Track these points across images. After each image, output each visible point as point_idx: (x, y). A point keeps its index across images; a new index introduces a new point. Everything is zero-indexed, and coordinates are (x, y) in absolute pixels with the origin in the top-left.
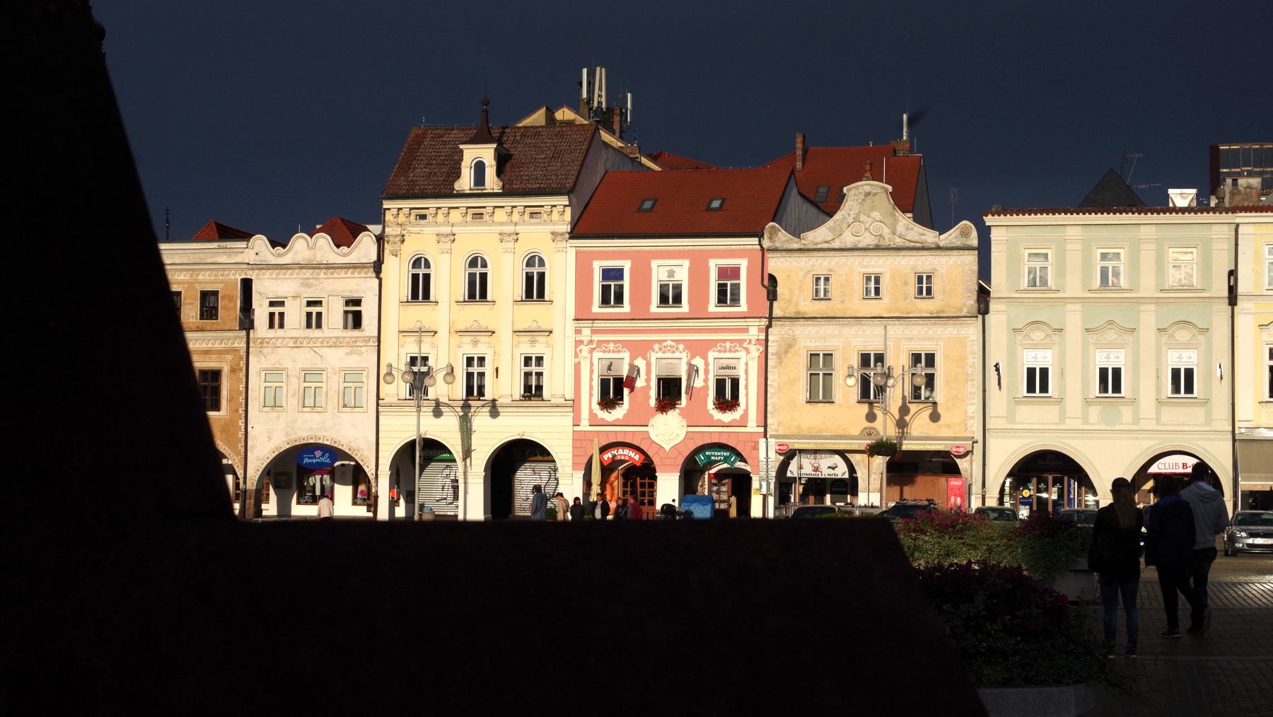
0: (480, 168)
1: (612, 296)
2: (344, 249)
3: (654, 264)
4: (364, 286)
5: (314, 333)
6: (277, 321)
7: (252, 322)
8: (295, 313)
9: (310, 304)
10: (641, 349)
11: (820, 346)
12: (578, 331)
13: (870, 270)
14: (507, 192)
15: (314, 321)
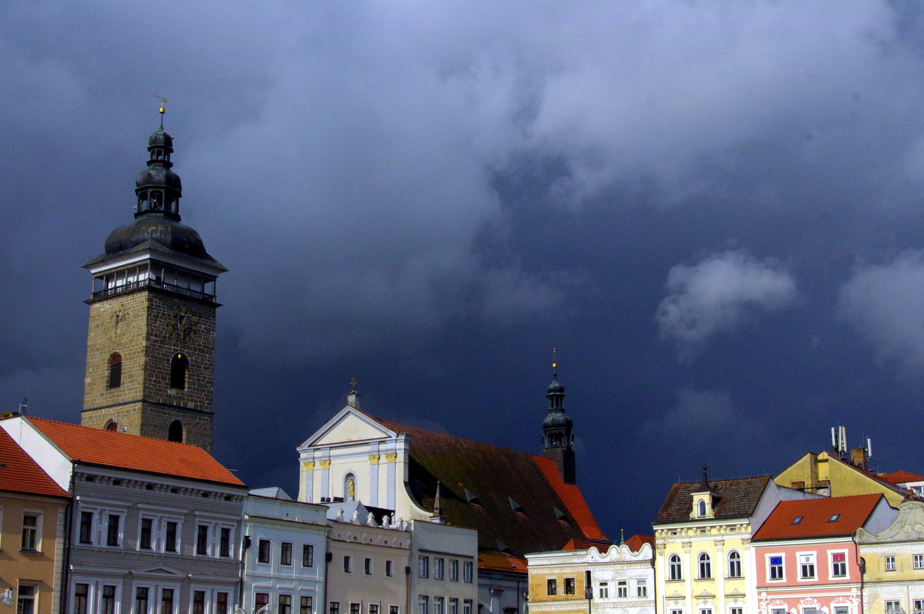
0: (703, 504)
1: (776, 573)
2: (636, 553)
3: (798, 554)
5: (623, 599)
6: (604, 594)
7: (591, 594)
8: (613, 589)
9: (620, 583)
10: (793, 603)
11: (892, 598)
12: (759, 594)
13: (916, 553)
14: (718, 517)
15: (622, 593)
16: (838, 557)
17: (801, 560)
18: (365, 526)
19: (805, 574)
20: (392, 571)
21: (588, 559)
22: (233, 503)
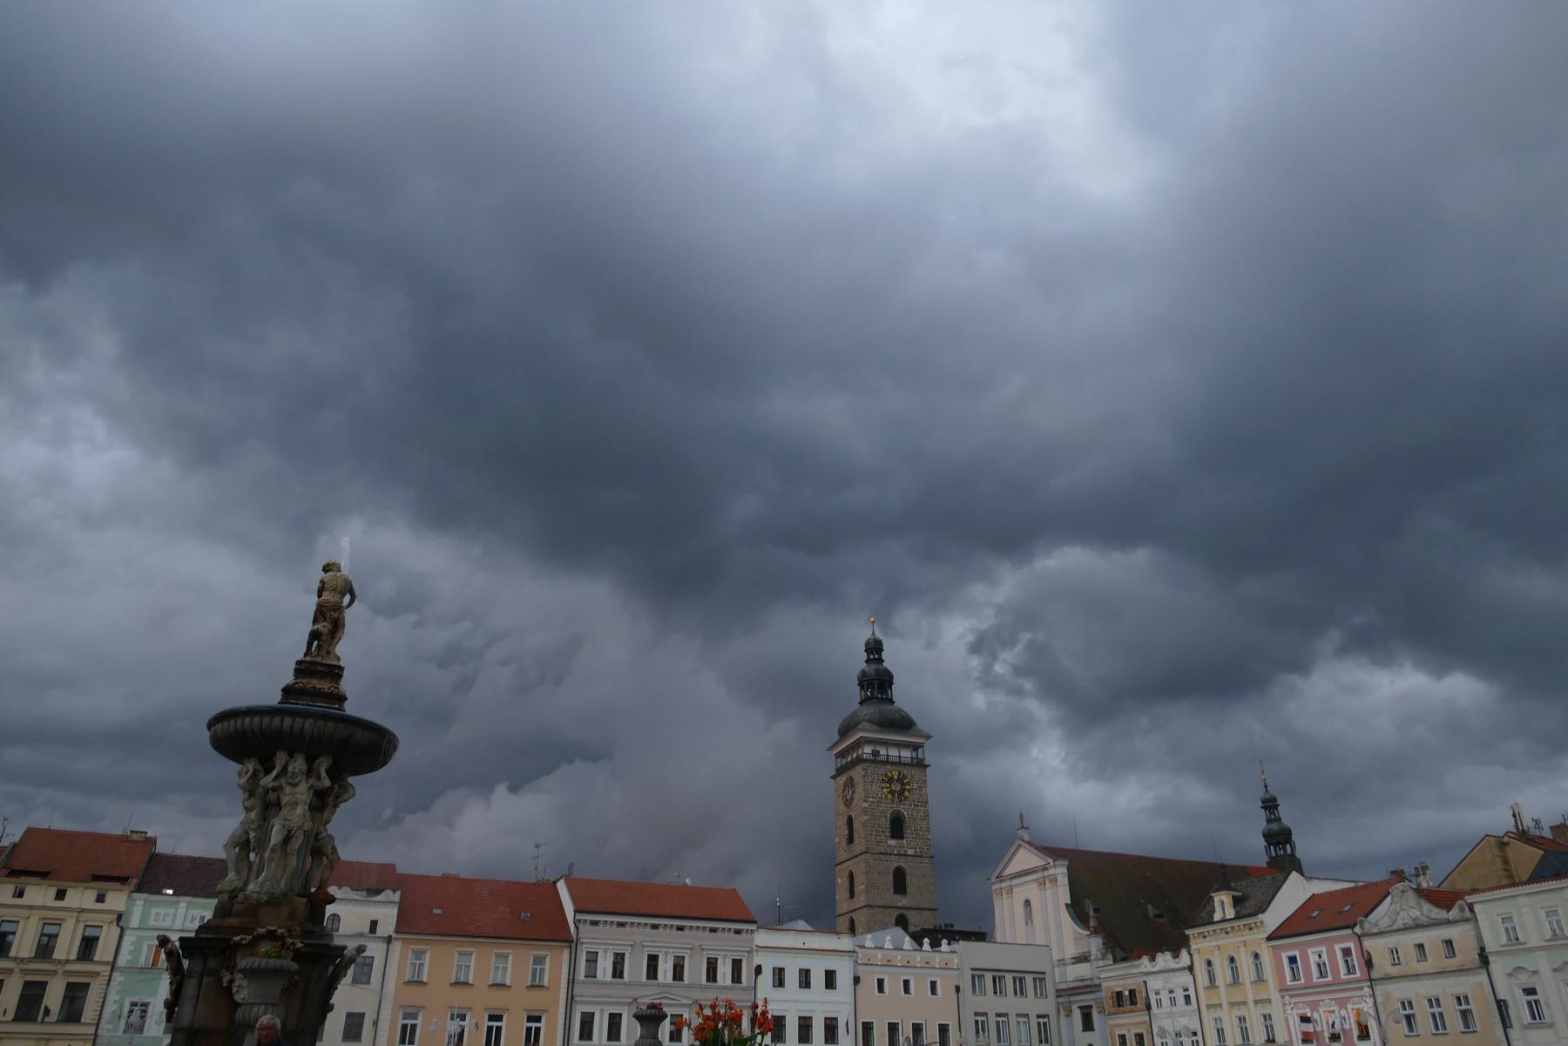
3: (1310, 951)
4: (1186, 979)
8: (1165, 997)
10: (1314, 1006)
14: (1237, 917)
15: (1173, 1001)
16: (1347, 952)
17: (1313, 959)
21: (1142, 969)
22: (744, 935)
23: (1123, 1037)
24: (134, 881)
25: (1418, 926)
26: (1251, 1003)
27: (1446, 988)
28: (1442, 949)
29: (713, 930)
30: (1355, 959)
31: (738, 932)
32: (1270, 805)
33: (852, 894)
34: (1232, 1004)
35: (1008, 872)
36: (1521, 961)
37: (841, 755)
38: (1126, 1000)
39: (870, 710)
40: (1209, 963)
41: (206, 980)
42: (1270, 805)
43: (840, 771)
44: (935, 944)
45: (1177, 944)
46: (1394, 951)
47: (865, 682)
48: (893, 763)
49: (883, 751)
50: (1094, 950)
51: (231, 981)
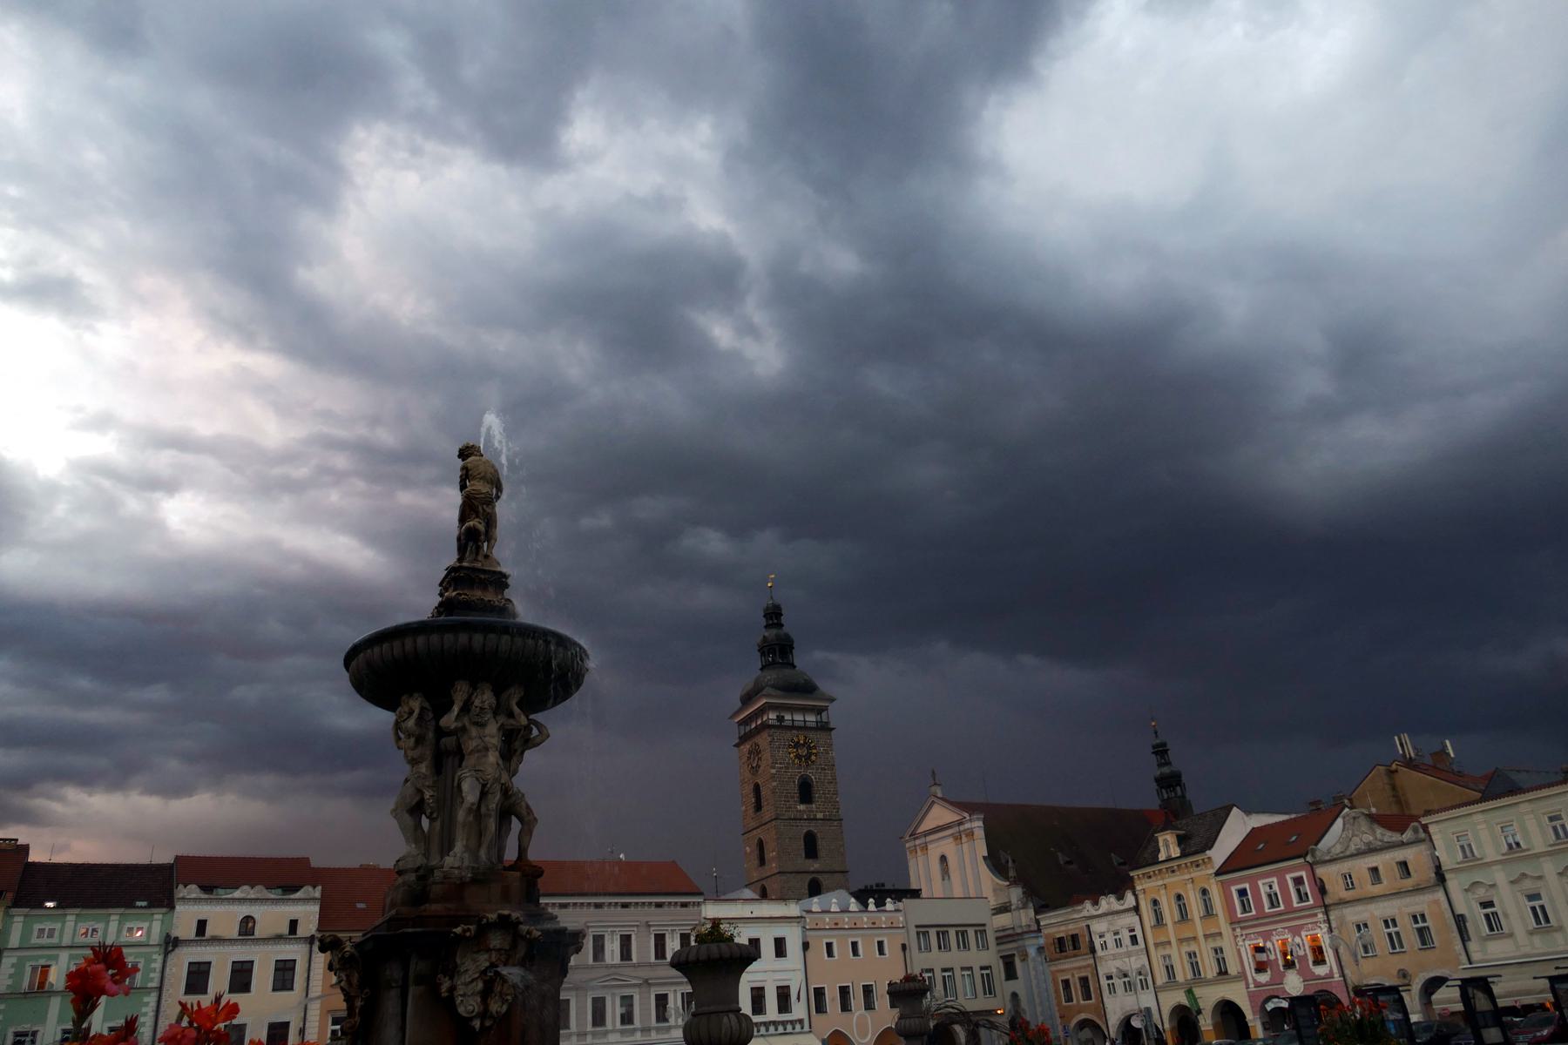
3: (1260, 883)
4: (1132, 919)
6: (1104, 946)
8: (1110, 939)
10: (1267, 936)
14: (1184, 855)
15: (1118, 943)
16: (1298, 881)
18: (845, 911)
19: (1272, 905)
20: (886, 950)
21: (1085, 913)
22: (691, 908)
23: (1066, 983)
24: (10, 896)
25: (1371, 850)
26: (1201, 939)
27: (1400, 908)
28: (1397, 872)
29: (659, 905)
30: (1307, 888)
31: (684, 905)
32: (1161, 751)
33: (762, 861)
34: (1181, 941)
35: (922, 828)
36: (1477, 876)
37: (740, 723)
38: (1069, 945)
39: (771, 676)
40: (1155, 902)
41: (413, 991)
42: (1161, 751)
43: (743, 739)
44: (880, 904)
45: (1120, 885)
46: (1347, 877)
47: (766, 648)
48: (799, 728)
49: (788, 717)
50: (1014, 900)
51: (452, 989)
